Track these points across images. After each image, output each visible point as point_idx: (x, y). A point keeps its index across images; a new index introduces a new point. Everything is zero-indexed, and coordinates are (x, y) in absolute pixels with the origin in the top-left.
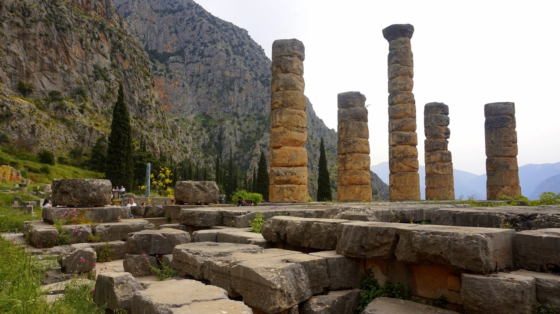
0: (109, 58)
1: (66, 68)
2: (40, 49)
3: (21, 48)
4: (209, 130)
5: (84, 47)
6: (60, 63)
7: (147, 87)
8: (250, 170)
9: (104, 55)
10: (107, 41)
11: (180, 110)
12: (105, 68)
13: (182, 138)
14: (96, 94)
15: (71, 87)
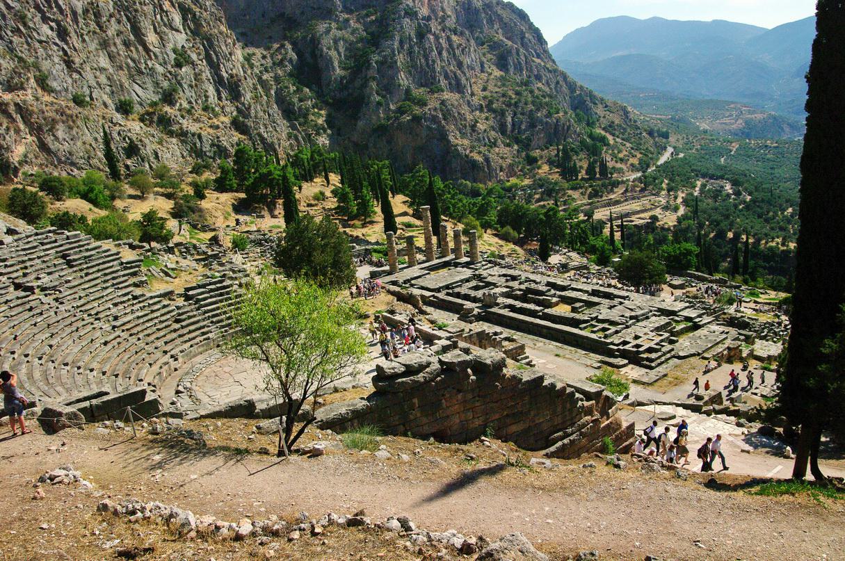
0: (183, 31)
1: (150, 66)
2: (121, 53)
3: (107, 60)
4: (294, 44)
5: (158, 30)
6: (143, 61)
7: (230, 54)
8: (367, 104)
9: (177, 31)
10: (175, 8)
11: (245, 15)
12: (183, 47)
13: (258, 64)
14: (185, 86)
15: (162, 88)
